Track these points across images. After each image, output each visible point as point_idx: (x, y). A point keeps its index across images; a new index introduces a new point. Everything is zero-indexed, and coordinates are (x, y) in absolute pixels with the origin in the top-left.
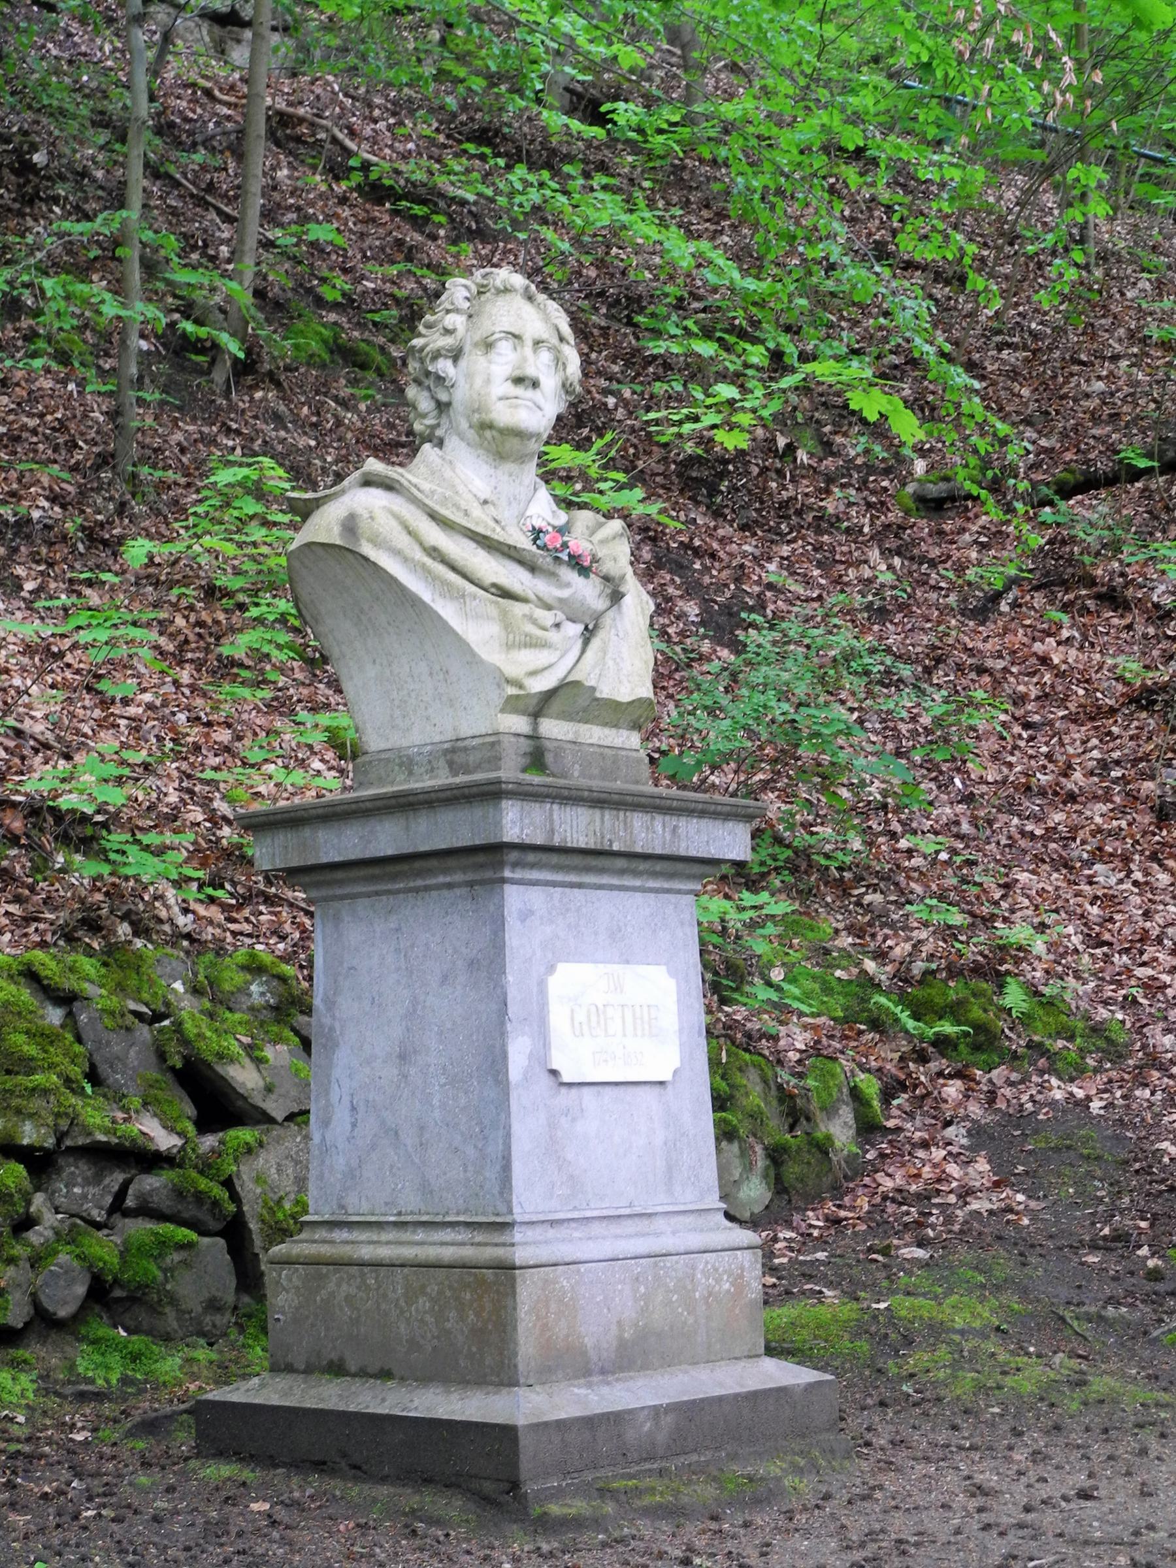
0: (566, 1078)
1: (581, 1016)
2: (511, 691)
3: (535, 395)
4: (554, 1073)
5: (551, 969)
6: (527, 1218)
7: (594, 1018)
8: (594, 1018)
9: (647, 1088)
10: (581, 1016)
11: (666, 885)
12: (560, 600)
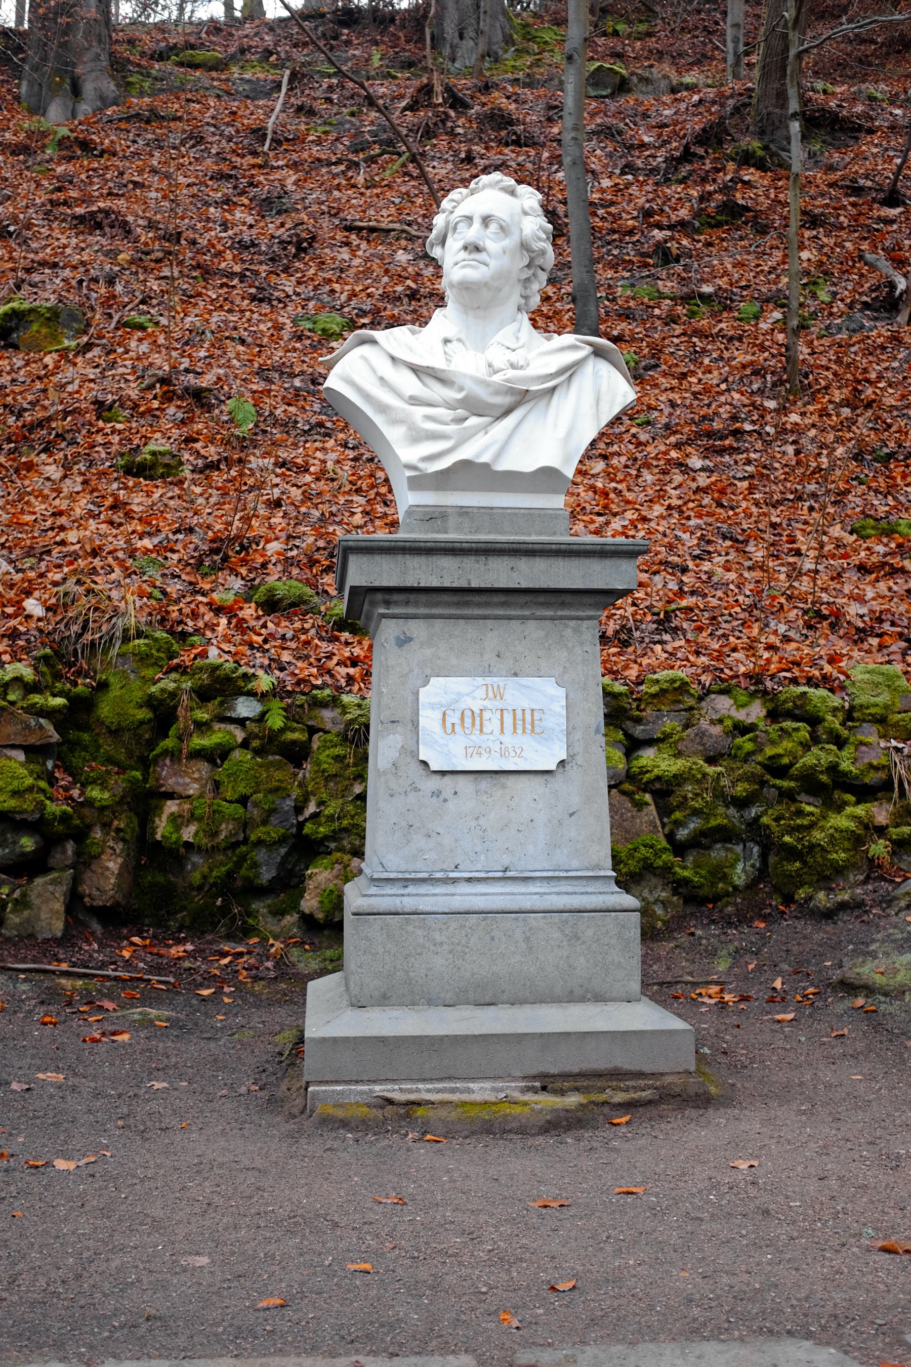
0: (434, 767)
1: (453, 718)
2: (409, 473)
3: (483, 256)
4: (425, 763)
5: (426, 683)
6: (385, 875)
7: (468, 721)
8: (468, 721)
9: (531, 777)
10: (453, 718)
11: (458, 612)
12: (458, 401)
